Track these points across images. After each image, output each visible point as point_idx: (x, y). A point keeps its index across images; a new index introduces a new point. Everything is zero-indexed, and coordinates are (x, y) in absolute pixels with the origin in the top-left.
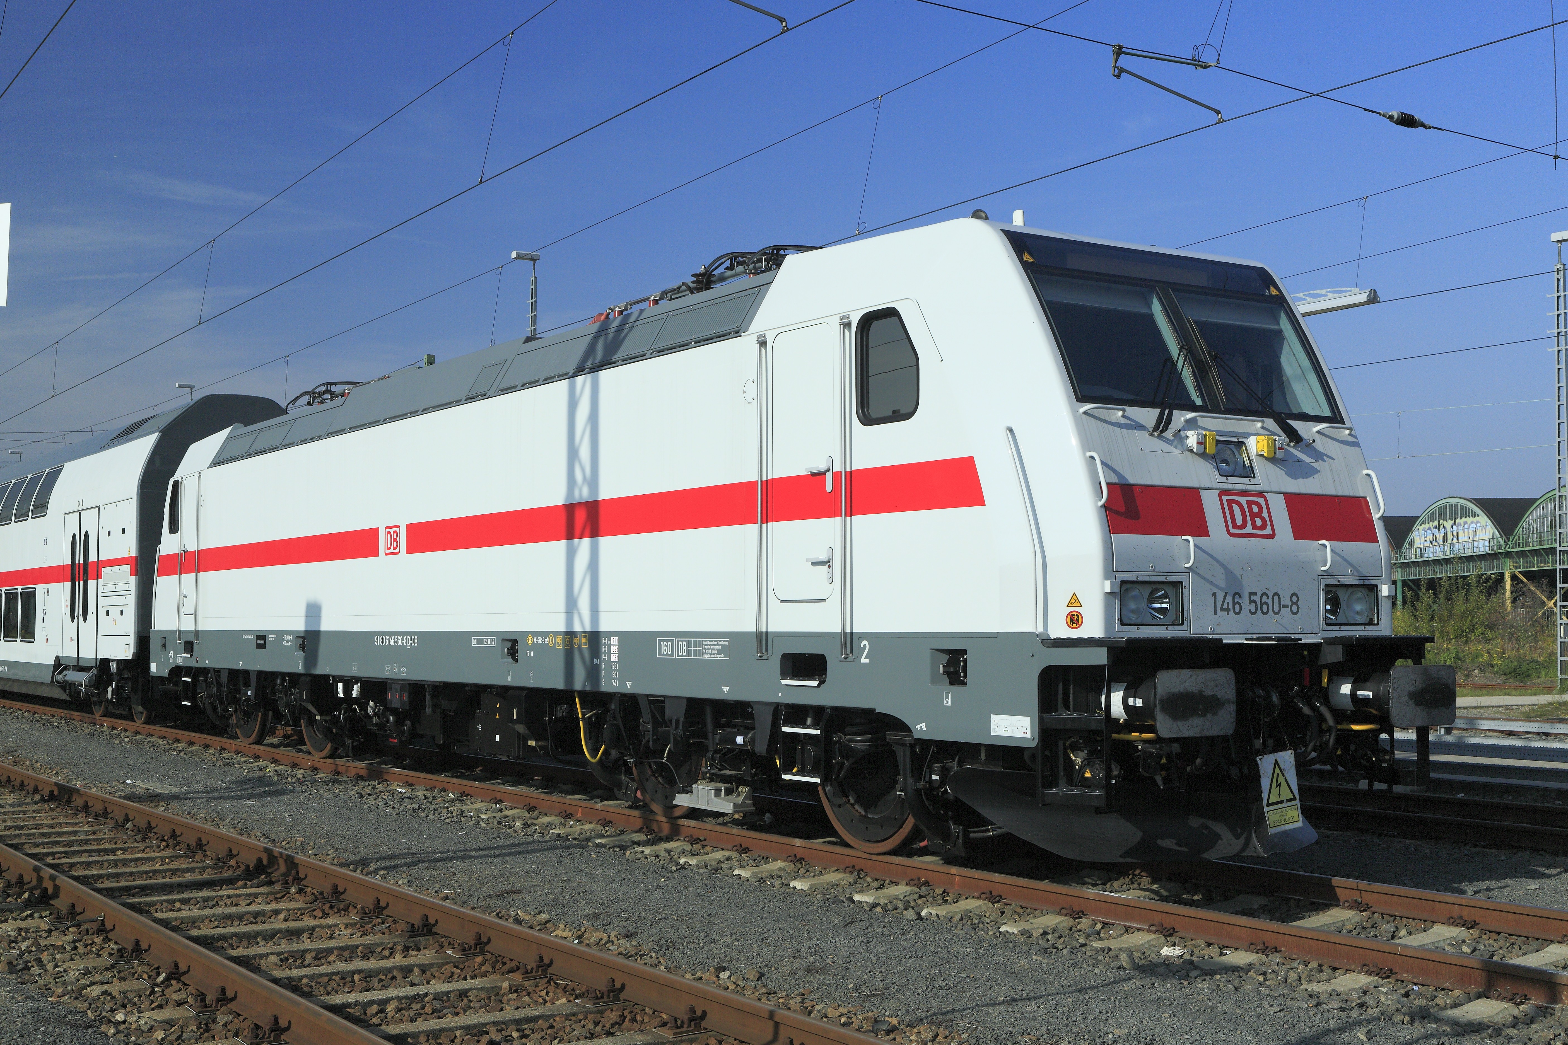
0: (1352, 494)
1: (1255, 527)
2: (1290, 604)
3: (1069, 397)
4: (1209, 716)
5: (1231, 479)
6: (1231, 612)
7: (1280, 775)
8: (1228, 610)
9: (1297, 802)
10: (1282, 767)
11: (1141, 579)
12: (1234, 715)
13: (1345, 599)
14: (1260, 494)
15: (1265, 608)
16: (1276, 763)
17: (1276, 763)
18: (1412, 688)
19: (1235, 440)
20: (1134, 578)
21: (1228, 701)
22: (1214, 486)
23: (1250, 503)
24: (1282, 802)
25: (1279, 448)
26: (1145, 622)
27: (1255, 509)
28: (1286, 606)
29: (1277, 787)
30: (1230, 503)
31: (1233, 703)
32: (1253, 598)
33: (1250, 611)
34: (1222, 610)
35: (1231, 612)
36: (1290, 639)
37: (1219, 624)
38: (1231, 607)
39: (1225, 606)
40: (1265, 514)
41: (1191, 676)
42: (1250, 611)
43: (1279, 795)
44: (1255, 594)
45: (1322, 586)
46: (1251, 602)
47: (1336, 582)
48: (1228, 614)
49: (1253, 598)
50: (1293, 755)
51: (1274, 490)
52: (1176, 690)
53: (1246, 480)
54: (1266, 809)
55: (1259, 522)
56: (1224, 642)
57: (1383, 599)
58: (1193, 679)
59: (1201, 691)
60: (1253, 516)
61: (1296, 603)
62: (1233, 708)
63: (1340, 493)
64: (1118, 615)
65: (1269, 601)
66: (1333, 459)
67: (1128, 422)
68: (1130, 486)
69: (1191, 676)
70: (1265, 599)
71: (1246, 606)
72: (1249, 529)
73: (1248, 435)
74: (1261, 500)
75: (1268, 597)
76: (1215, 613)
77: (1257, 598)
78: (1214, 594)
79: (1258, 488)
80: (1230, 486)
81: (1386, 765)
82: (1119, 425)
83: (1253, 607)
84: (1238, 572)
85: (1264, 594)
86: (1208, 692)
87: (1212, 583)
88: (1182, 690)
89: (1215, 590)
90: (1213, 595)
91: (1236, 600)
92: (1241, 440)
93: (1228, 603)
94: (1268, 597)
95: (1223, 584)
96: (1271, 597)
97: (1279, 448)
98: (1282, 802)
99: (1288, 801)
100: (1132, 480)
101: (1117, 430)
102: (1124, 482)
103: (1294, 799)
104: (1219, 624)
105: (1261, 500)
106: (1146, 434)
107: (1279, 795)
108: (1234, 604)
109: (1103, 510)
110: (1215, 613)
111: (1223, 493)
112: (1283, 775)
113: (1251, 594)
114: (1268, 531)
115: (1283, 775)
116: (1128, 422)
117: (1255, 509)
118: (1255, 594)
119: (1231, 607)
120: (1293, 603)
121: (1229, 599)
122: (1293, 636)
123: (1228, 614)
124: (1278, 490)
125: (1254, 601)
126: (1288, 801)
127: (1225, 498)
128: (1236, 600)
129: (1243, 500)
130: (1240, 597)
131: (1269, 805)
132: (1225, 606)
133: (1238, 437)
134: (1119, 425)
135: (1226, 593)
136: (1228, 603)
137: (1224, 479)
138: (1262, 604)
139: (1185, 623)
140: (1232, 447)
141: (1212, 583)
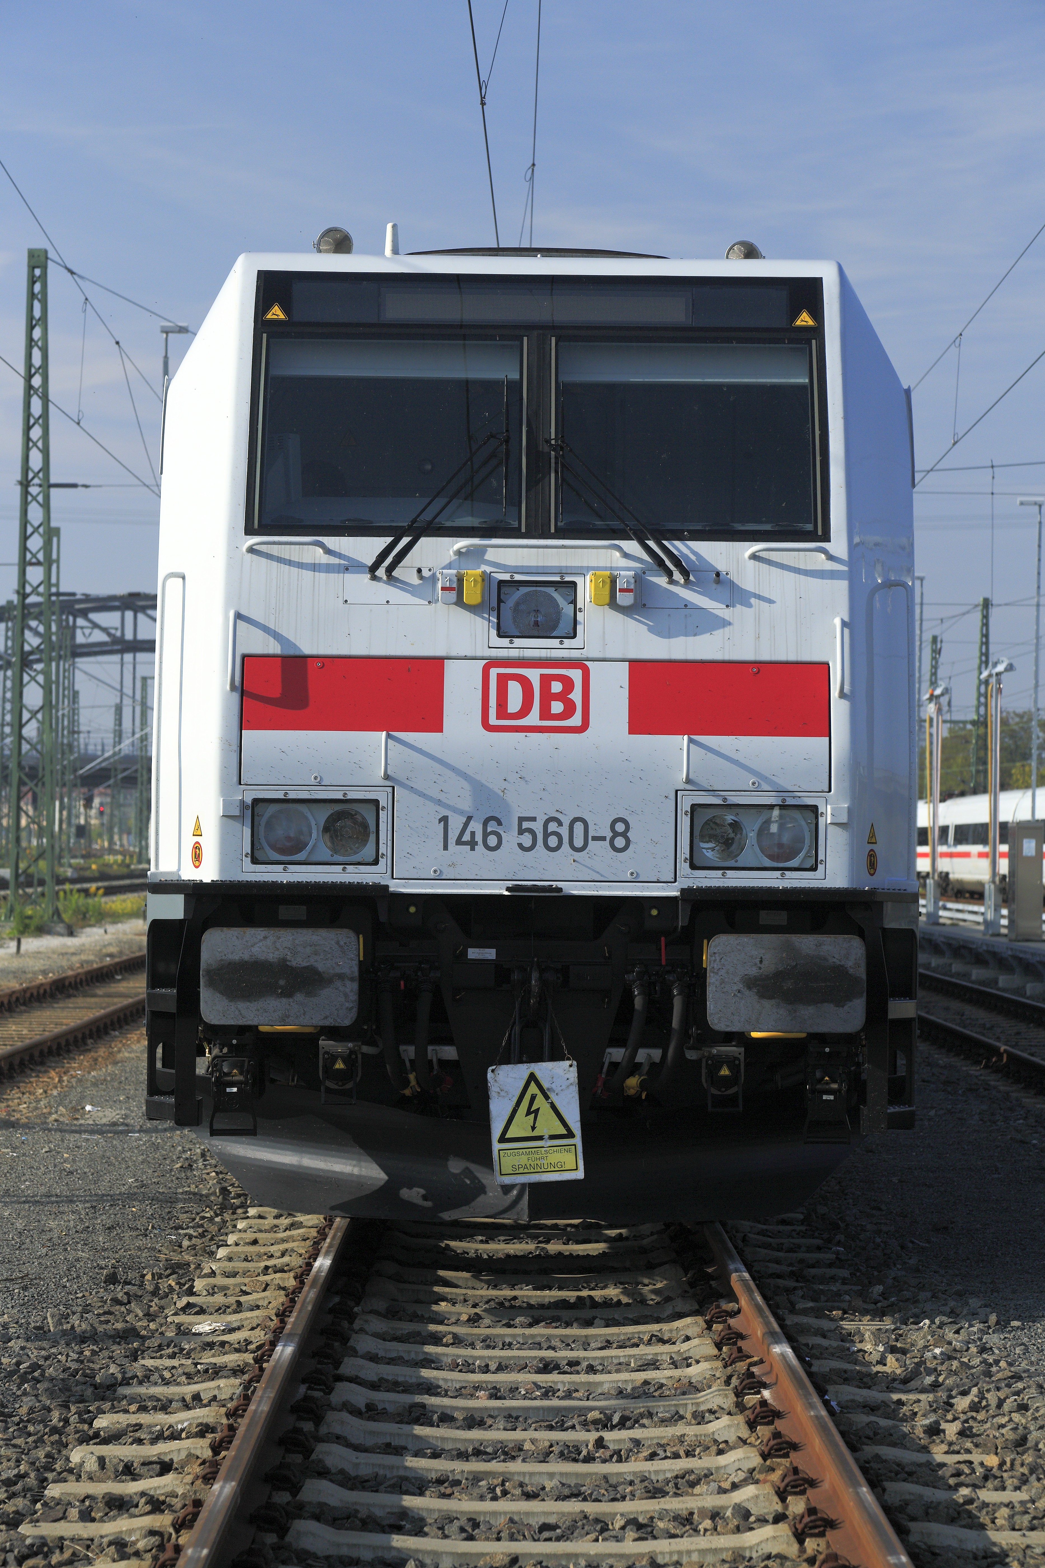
0: (792, 657)
1: (545, 713)
2: (609, 834)
3: (232, 528)
4: (299, 997)
5: (518, 642)
6: (480, 847)
7: (540, 1096)
8: (472, 844)
9: (578, 1140)
10: (545, 1085)
11: (292, 795)
12: (354, 997)
13: (756, 827)
14: (578, 664)
15: (553, 841)
16: (532, 1077)
17: (532, 1077)
18: (753, 971)
19: (558, 579)
20: (280, 795)
21: (341, 977)
22: (479, 654)
23: (546, 681)
24: (540, 1138)
25: (621, 590)
26: (314, 859)
27: (557, 687)
28: (603, 839)
29: (528, 1113)
30: (503, 681)
31: (352, 979)
32: (525, 825)
33: (520, 846)
34: (459, 842)
35: (480, 847)
36: (550, 889)
37: (453, 865)
38: (479, 838)
39: (467, 837)
40: (576, 696)
41: (265, 938)
42: (520, 846)
43: (533, 1128)
44: (534, 819)
45: (685, 805)
46: (521, 832)
47: (720, 802)
48: (473, 849)
49: (525, 825)
50: (574, 1070)
51: (609, 655)
52: (236, 957)
53: (555, 643)
54: (496, 1146)
55: (557, 707)
56: (391, 889)
57: (831, 829)
58: (269, 942)
59: (284, 960)
60: (547, 697)
61: (624, 835)
62: (351, 988)
63: (765, 655)
64: (247, 848)
65: (564, 832)
66: (770, 601)
67: (336, 561)
68: (304, 659)
69: (265, 938)
70: (552, 827)
71: (511, 838)
72: (533, 718)
73: (581, 572)
74: (576, 675)
75: (560, 824)
76: (446, 848)
77: (537, 827)
78: (444, 820)
79: (575, 654)
80: (514, 653)
81: (832, 1097)
82: (315, 567)
83: (527, 840)
84: (496, 786)
85: (552, 819)
86: (298, 962)
87: (439, 802)
88: (246, 957)
89: (445, 812)
90: (440, 821)
91: (489, 829)
92: (567, 579)
93: (473, 834)
94: (560, 824)
95: (466, 805)
96: (566, 822)
97: (621, 590)
98: (540, 1138)
99: (553, 1137)
100: (307, 649)
101: (308, 574)
102: (291, 652)
103: (570, 1135)
104: (453, 865)
105: (576, 675)
106: (365, 578)
107: (533, 1128)
108: (486, 835)
109: (236, 696)
110: (446, 848)
111: (493, 662)
112: (547, 1097)
113: (521, 820)
114: (576, 720)
115: (547, 1097)
116: (336, 561)
117: (557, 687)
118: (534, 819)
119: (479, 838)
120: (616, 834)
121: (476, 826)
122: (554, 884)
123: (473, 849)
124: (619, 656)
125: (531, 831)
126: (553, 1137)
127: (494, 672)
128: (489, 829)
129: (534, 675)
130: (500, 823)
131: (503, 1139)
132: (467, 837)
133: (562, 574)
134: (315, 567)
135: (469, 819)
136: (473, 834)
137: (505, 642)
138: (546, 835)
139: (382, 861)
140: (551, 591)
141: (439, 802)
